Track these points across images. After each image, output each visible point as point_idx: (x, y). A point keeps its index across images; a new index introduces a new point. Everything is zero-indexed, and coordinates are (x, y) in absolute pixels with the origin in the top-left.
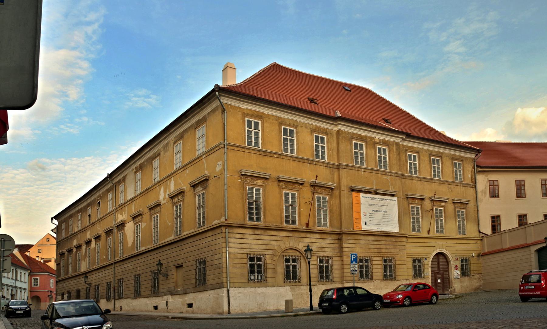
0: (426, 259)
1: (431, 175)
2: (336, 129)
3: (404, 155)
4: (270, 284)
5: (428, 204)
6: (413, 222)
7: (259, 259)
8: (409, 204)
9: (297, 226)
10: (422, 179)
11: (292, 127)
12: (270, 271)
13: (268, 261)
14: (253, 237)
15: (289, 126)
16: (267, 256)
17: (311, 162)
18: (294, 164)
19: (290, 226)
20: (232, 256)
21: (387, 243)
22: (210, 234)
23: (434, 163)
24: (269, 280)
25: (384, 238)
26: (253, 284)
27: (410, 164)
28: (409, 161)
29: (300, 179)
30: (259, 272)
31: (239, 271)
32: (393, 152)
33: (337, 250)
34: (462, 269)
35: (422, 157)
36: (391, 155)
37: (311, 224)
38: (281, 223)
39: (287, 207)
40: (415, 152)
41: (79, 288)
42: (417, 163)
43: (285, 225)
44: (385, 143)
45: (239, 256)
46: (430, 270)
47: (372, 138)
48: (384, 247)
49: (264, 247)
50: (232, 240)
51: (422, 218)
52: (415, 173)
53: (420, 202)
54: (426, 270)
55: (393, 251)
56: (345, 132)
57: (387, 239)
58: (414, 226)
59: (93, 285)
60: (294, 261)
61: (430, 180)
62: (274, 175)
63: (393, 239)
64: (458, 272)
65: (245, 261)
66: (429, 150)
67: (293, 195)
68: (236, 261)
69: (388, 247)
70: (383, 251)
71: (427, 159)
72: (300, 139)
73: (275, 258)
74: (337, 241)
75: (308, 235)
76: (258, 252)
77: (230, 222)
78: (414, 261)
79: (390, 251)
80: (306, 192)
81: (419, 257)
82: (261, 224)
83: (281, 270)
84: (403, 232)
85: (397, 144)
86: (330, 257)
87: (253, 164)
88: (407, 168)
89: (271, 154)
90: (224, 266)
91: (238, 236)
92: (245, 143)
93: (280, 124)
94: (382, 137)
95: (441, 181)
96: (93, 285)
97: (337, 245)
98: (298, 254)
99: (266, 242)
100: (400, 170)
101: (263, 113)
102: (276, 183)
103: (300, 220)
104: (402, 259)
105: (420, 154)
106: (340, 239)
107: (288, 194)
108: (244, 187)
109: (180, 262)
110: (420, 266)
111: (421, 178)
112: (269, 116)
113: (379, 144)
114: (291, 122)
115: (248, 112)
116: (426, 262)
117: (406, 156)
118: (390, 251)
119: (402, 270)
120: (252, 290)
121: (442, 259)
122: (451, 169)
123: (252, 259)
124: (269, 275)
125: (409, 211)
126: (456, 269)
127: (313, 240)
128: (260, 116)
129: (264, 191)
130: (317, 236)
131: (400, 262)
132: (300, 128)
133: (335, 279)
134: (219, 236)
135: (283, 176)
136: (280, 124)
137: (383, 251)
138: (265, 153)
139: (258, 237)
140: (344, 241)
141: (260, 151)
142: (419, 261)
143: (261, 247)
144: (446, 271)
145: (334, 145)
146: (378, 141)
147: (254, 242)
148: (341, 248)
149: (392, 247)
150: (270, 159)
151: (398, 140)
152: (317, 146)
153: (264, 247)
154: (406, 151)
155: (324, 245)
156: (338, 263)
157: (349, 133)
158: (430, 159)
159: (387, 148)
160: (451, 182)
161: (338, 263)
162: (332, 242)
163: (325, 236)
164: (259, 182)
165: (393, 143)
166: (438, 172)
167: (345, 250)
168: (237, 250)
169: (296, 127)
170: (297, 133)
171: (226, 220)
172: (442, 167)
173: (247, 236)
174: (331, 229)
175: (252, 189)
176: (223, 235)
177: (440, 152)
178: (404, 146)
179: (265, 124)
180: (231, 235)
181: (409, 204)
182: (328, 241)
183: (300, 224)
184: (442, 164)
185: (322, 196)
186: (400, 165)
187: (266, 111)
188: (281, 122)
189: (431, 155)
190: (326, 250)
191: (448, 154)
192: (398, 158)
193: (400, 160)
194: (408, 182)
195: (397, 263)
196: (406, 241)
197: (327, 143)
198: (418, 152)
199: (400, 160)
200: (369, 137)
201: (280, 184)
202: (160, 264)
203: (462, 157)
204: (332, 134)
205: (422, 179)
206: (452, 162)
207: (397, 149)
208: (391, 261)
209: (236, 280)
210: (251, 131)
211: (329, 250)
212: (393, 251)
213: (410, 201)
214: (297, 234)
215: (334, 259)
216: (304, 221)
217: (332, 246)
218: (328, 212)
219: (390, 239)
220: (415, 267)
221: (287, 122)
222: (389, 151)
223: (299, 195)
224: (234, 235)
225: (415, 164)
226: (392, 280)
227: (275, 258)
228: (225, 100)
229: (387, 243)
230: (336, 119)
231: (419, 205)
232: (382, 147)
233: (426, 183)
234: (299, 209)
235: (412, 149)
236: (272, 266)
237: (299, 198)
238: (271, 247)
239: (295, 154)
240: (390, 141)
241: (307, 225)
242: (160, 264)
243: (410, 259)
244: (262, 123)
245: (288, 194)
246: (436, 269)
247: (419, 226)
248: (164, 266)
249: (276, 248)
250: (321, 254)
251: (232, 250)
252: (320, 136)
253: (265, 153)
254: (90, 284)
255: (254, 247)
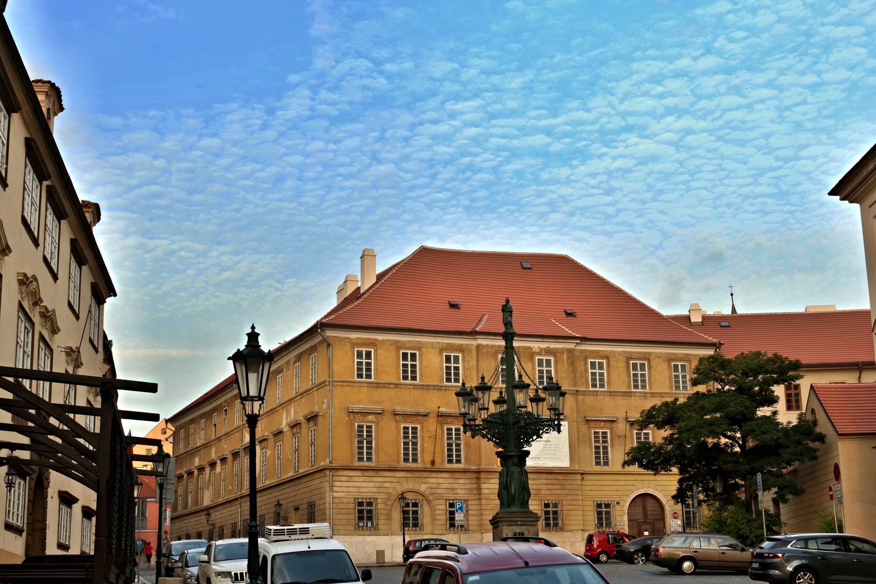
0: (618, 503)
1: (629, 387)
2: (475, 343)
3: (583, 363)
4: (383, 532)
5: (622, 427)
6: (597, 453)
7: (370, 504)
8: (589, 428)
9: (419, 465)
10: (612, 394)
11: (414, 349)
12: (382, 517)
13: (380, 506)
14: (363, 479)
15: (410, 349)
16: (379, 501)
17: (439, 388)
18: (417, 392)
19: (410, 465)
20: (337, 500)
21: (550, 482)
22: (318, 475)
23: (635, 368)
24: (381, 527)
25: (544, 476)
26: (361, 532)
27: (594, 374)
28: (590, 371)
29: (422, 410)
30: (370, 518)
31: (345, 517)
32: (563, 361)
33: (475, 492)
34: (688, 518)
35: (613, 363)
36: (559, 367)
37: (437, 461)
38: (398, 462)
39: (406, 444)
40: (602, 358)
41: (201, 529)
42: (605, 371)
43: (403, 464)
44: (548, 351)
45: (345, 500)
46: (626, 518)
47: (530, 348)
48: (545, 487)
49: (375, 490)
50: (337, 484)
51: (612, 446)
52: (602, 386)
53: (608, 425)
54: (618, 518)
55: (558, 492)
56: (487, 346)
57: (549, 476)
58: (597, 458)
59: (217, 525)
60: (415, 505)
61: (627, 394)
62: (388, 407)
63: (560, 477)
64: (679, 522)
65: (352, 506)
66: (625, 352)
67: (414, 429)
68: (342, 506)
69: (551, 487)
70: (543, 492)
71: (622, 364)
72: (424, 363)
73: (389, 503)
74: (474, 481)
75: (434, 475)
76: (369, 495)
77: (334, 465)
78: (599, 506)
79: (554, 492)
80: (432, 424)
81: (605, 500)
82: (372, 464)
83: (397, 516)
84: (576, 467)
85: (569, 351)
86: (465, 500)
87: (362, 398)
88: (587, 381)
89: (386, 385)
90: (328, 513)
91: (344, 479)
92: (354, 376)
93: (398, 349)
94: (544, 345)
95: (645, 393)
96: (217, 525)
97: (475, 486)
98: (420, 497)
99: (378, 485)
100: (575, 384)
101: (376, 340)
102: (391, 417)
103: (423, 457)
104: (575, 502)
105: (611, 359)
106: (478, 478)
107: (408, 428)
108: (352, 425)
109: (297, 503)
110: (608, 513)
111: (610, 392)
112: (383, 342)
113: (540, 354)
114: (412, 345)
115: (359, 341)
116: (618, 507)
117: (586, 364)
118: (554, 492)
119: (574, 518)
120: (361, 538)
121: (650, 504)
122: (667, 374)
123: (360, 504)
124: (381, 522)
125: (590, 437)
126: (675, 518)
127: (441, 481)
128: (373, 343)
129: (377, 426)
130: (446, 475)
131: (571, 507)
132: (424, 350)
133: (471, 528)
134: (324, 479)
135: (398, 409)
136: (398, 349)
137: (543, 492)
138: (378, 385)
139: (368, 479)
140: (482, 480)
141: (372, 383)
142: (607, 506)
143: (371, 490)
144: (660, 520)
145: (473, 362)
146: (538, 351)
147: (364, 484)
148: (479, 489)
149: (558, 487)
150: (385, 390)
151: (572, 346)
152: (448, 368)
153: (375, 490)
154: (586, 358)
155: (456, 486)
156: (476, 507)
157: (493, 346)
158: (628, 364)
159: (552, 359)
160: (666, 393)
161: (476, 507)
162: (468, 481)
163: (457, 475)
164: (370, 417)
165: (562, 351)
166: (643, 381)
167: (484, 491)
168: (342, 495)
169: (419, 349)
170: (421, 355)
171: (331, 462)
172: (649, 373)
173: (355, 479)
174: (467, 467)
175: (362, 427)
176: (327, 478)
177: (645, 353)
178: (582, 351)
179: (379, 352)
180: (336, 478)
181: (589, 428)
182: (462, 481)
183: (423, 461)
184: (650, 369)
185: (453, 427)
186: (575, 378)
187: (380, 337)
188: (398, 345)
189: (628, 359)
190: (459, 491)
191: (661, 353)
192: (571, 369)
193: (574, 371)
194: (589, 399)
195: (565, 508)
196: (582, 479)
197: (463, 361)
198: (607, 357)
199: (574, 371)
200: (523, 347)
201: (397, 418)
202: (279, 505)
203: (688, 355)
204: (470, 350)
205: (612, 394)
206: (669, 365)
207: (568, 358)
208: (555, 505)
209: (341, 527)
210: (362, 363)
211: (463, 492)
212: (558, 492)
213: (592, 424)
214: (418, 474)
215: (470, 502)
216: (429, 458)
217: (468, 486)
218: (462, 446)
219: (553, 476)
220: (599, 513)
221: (408, 345)
222: (556, 362)
223: (422, 428)
224: (340, 478)
225: (601, 374)
226: (557, 530)
227: (389, 503)
228: (330, 333)
229: (550, 482)
230: (473, 334)
231: (607, 428)
232: (545, 358)
233: (619, 398)
234: (422, 445)
235: (597, 354)
236: (386, 512)
237: (422, 431)
238: (385, 490)
239: (418, 382)
240: (557, 349)
241: (433, 463)
242: (279, 505)
243: (591, 503)
244: (376, 351)
245: (408, 428)
246: (640, 517)
247: (607, 457)
248: (283, 507)
249: (390, 490)
250: (452, 497)
251: (335, 495)
252: (452, 354)
253: (378, 385)
254: (213, 525)
255: (363, 490)
